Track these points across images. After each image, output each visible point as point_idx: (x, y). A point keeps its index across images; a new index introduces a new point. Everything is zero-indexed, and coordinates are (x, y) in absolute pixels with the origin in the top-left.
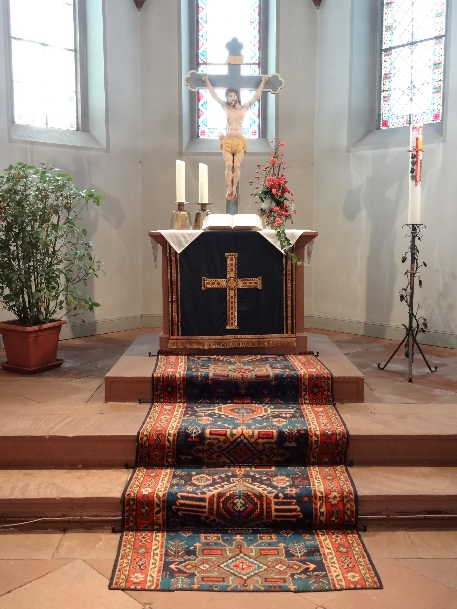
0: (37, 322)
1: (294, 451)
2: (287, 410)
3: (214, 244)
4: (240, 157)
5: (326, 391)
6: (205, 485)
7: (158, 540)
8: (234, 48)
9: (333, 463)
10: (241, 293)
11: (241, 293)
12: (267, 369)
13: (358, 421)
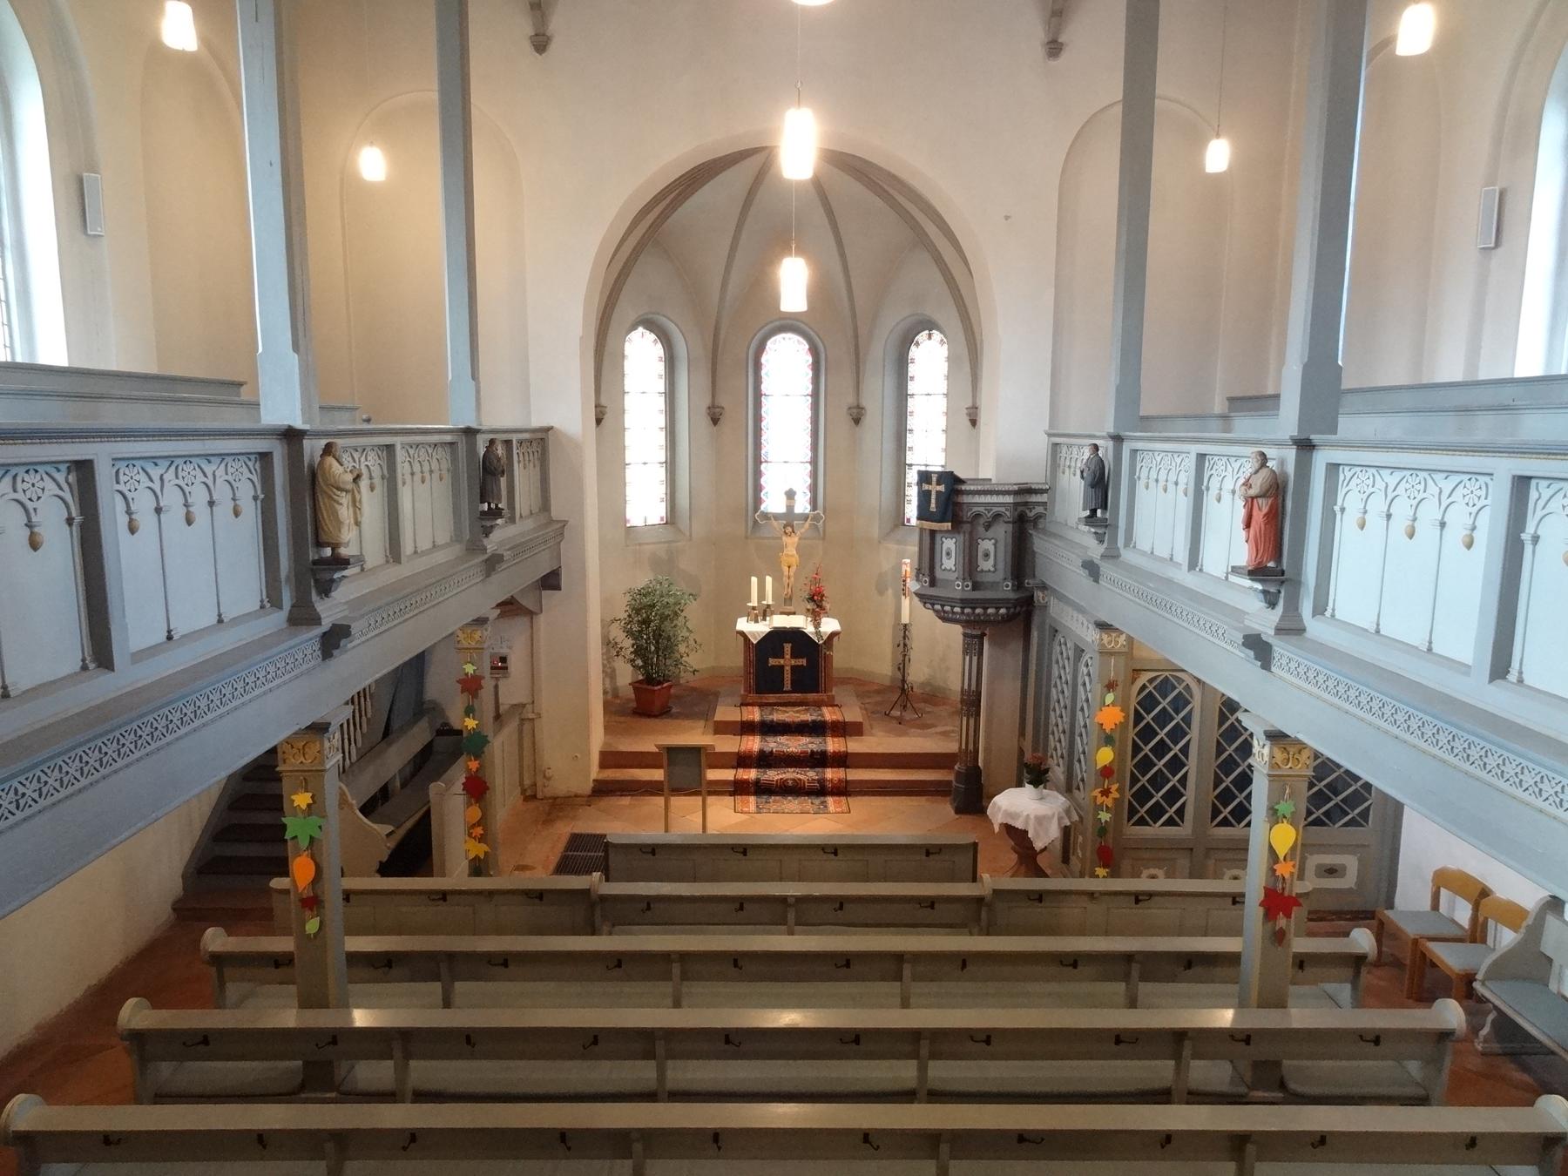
0: (660, 683)
1: (819, 760)
2: (818, 740)
3: (778, 636)
4: (793, 569)
5: (842, 729)
6: (773, 775)
7: (752, 799)
8: (790, 495)
9: (839, 766)
10: (793, 668)
11: (793, 668)
12: (808, 717)
13: (855, 746)
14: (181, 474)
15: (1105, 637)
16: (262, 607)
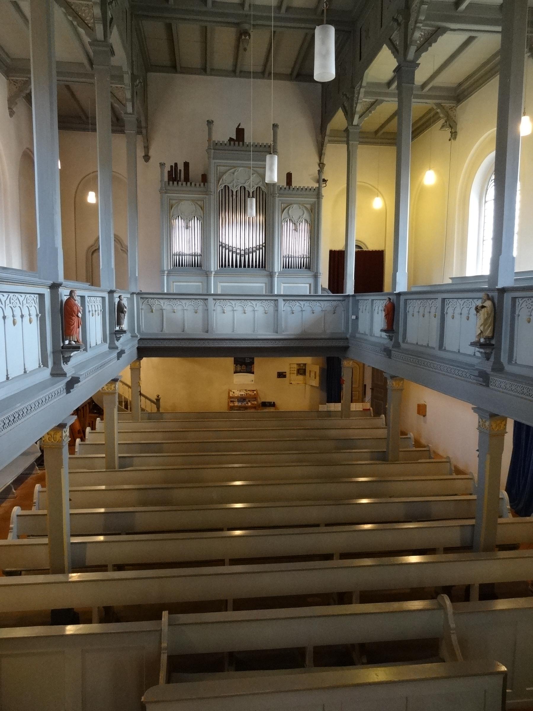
14: (12, 301)
15: (394, 383)
16: (40, 367)
